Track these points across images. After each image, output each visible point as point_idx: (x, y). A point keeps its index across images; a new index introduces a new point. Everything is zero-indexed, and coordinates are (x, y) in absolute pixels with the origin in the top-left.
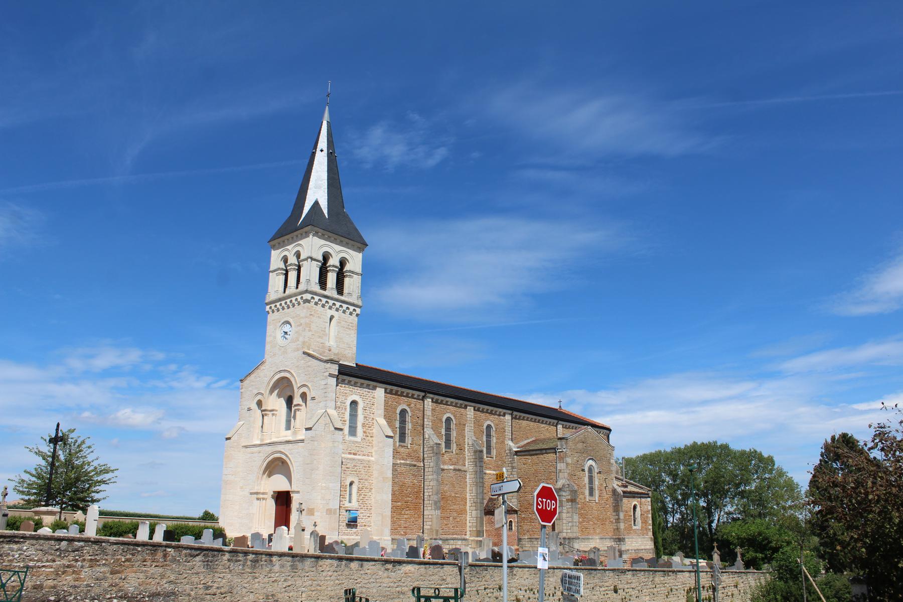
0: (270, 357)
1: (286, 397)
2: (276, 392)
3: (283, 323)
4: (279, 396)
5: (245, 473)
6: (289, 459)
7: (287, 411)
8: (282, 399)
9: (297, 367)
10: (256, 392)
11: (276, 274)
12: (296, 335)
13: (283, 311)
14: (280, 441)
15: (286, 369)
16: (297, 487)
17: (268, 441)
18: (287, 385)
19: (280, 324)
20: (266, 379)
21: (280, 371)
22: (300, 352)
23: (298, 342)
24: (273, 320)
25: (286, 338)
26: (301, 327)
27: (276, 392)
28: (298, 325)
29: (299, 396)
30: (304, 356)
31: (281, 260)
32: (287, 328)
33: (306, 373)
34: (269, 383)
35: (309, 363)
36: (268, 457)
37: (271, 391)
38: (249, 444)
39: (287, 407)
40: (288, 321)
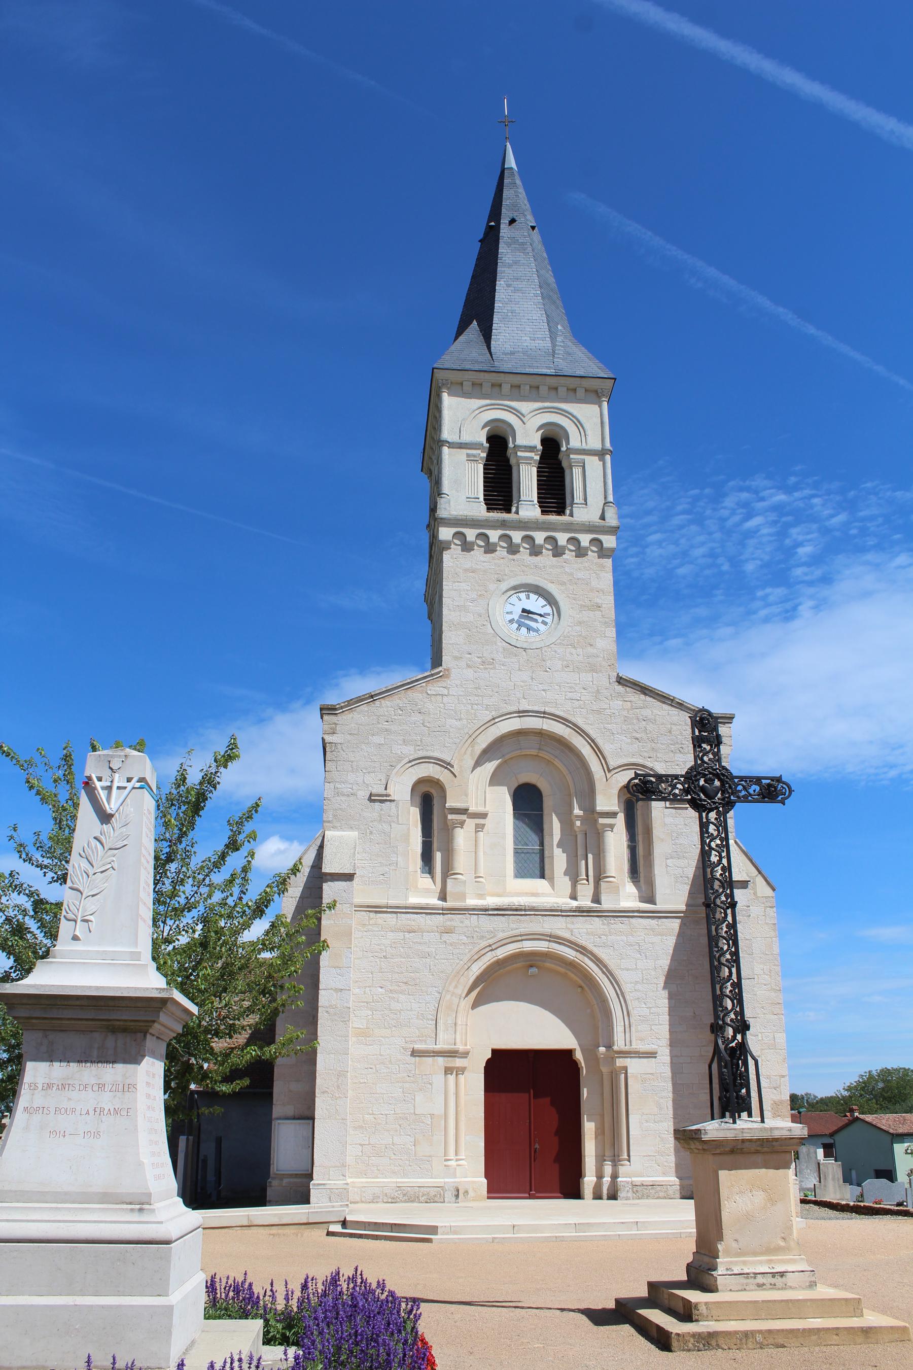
0: (468, 666)
1: (516, 785)
2: (490, 767)
3: (514, 588)
4: (495, 779)
5: (380, 990)
6: (598, 961)
7: (514, 822)
8: (506, 788)
9: (599, 712)
10: (410, 752)
11: (468, 455)
12: (578, 628)
13: (511, 557)
14: (548, 906)
15: (548, 710)
16: (642, 1040)
17: (491, 901)
18: (534, 752)
19: (504, 589)
20: (458, 724)
21: (522, 713)
22: (605, 680)
23: (590, 650)
24: (466, 570)
25: (529, 629)
26: (598, 613)
27: (490, 767)
28: (582, 606)
29: (615, 791)
30: (620, 688)
31: (483, 427)
32: (536, 604)
33: (638, 736)
34: (472, 738)
35: (647, 712)
36: (491, 948)
37: (478, 763)
38: (392, 902)
39: (514, 814)
40: (537, 587)
